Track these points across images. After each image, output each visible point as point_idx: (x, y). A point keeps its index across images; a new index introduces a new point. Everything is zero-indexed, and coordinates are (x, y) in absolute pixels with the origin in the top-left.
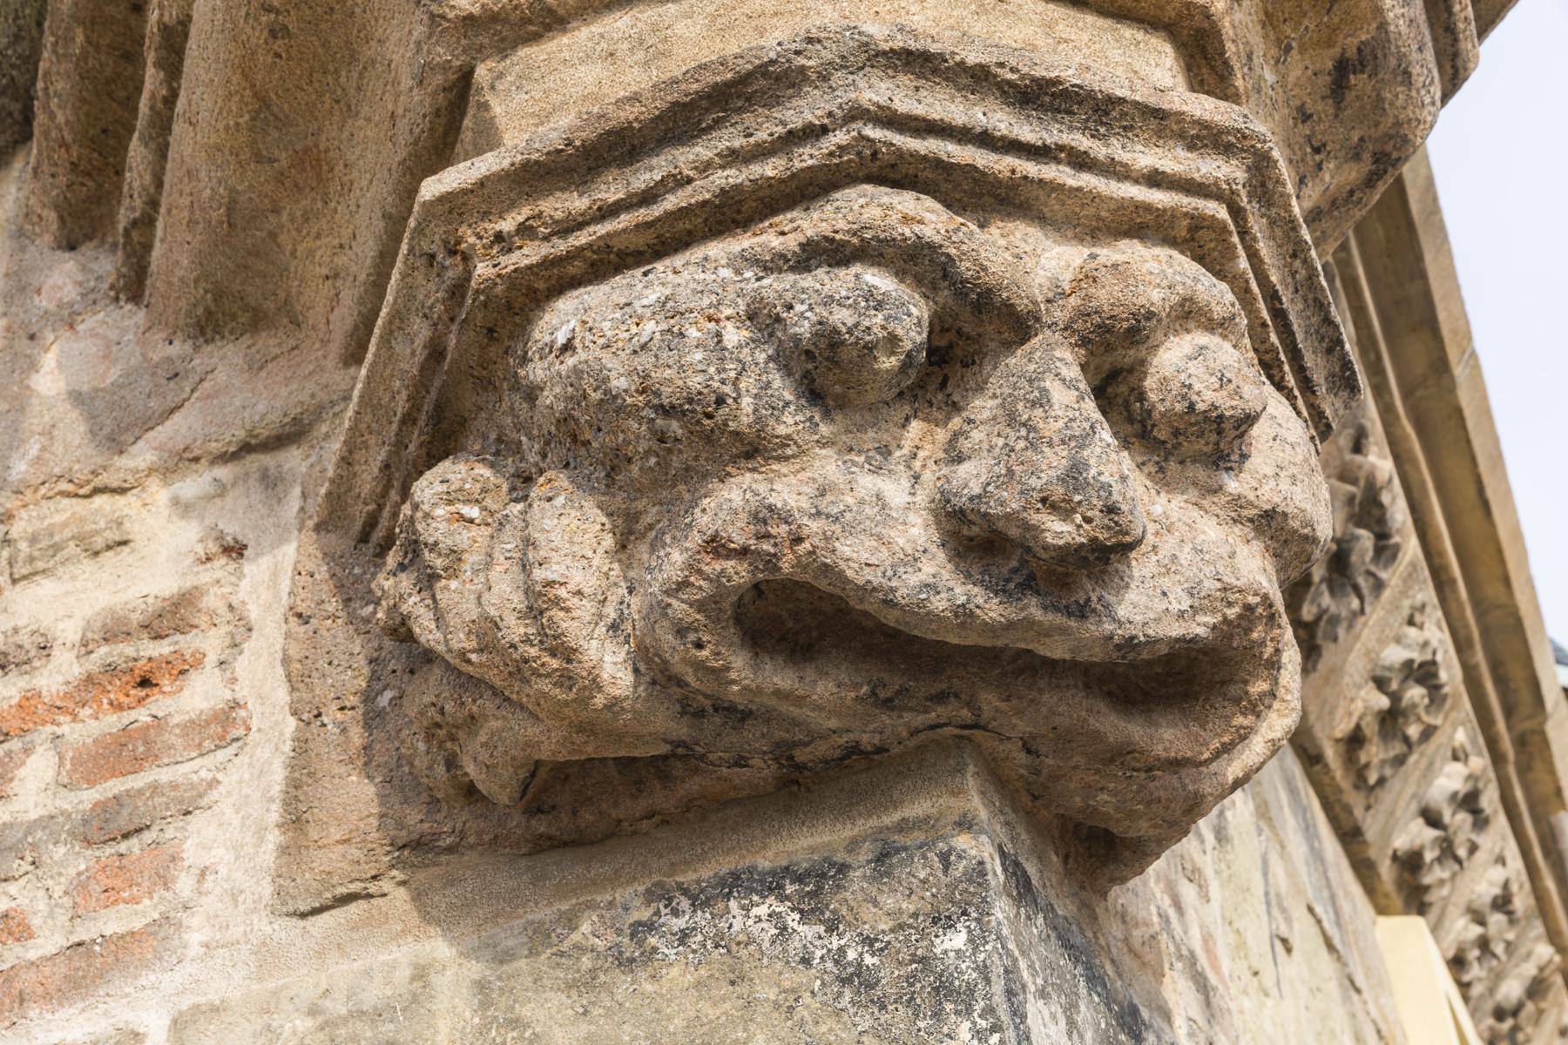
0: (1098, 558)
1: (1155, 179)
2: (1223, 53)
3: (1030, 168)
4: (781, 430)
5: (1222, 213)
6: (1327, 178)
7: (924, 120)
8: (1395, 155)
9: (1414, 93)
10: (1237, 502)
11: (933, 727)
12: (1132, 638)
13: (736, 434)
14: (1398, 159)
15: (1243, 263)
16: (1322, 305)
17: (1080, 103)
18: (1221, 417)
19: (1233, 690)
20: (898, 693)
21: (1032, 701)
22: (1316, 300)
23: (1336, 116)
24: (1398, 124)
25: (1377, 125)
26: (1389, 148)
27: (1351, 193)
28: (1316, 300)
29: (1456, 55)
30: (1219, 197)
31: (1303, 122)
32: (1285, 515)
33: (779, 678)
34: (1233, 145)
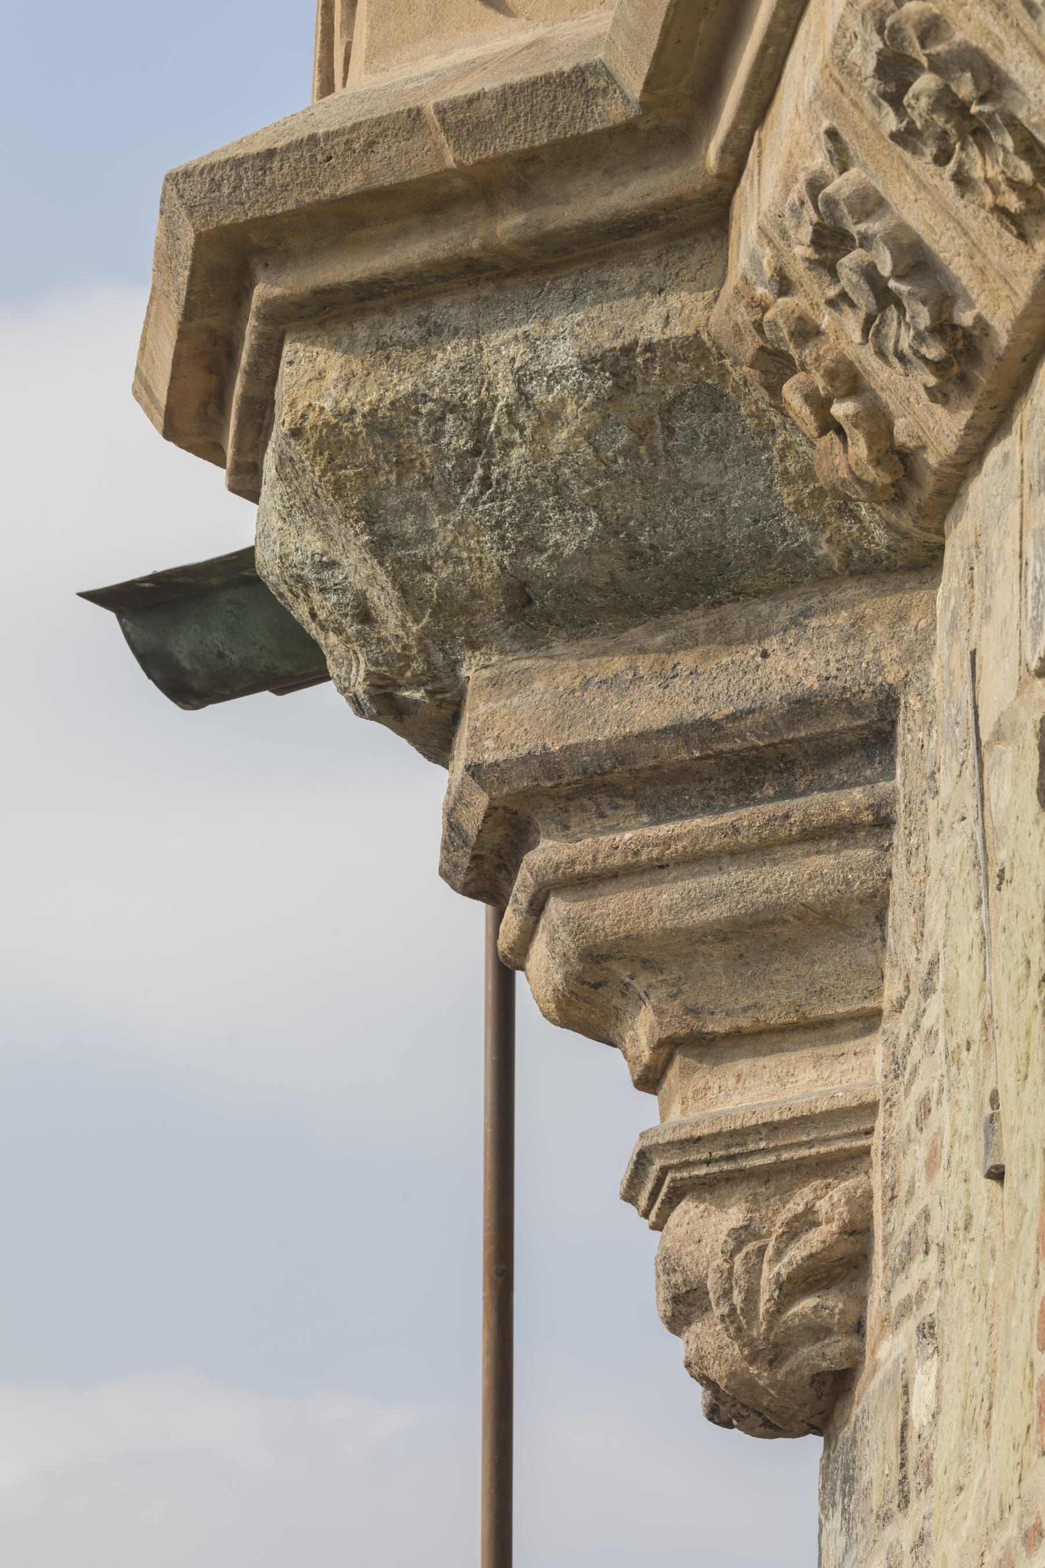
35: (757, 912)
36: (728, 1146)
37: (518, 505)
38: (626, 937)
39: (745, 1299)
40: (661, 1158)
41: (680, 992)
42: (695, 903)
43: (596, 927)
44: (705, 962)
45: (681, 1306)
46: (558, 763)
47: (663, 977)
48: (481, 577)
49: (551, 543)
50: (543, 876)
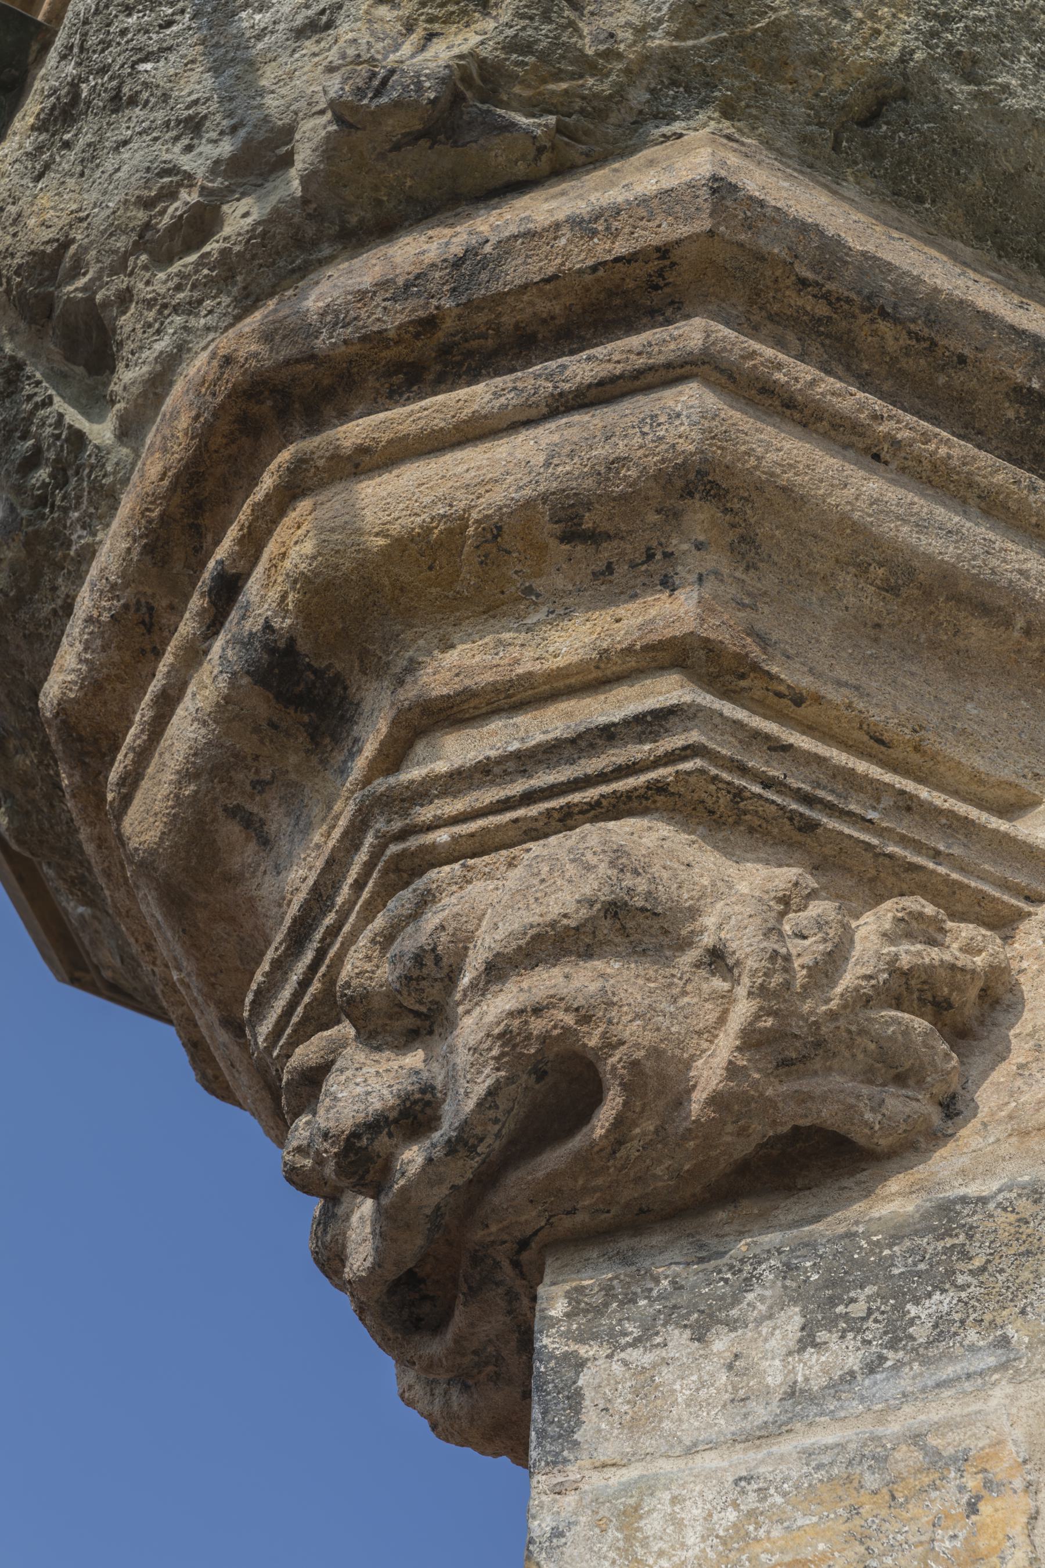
0: (356, 1154)
1: (359, 886)
2: (449, 696)
3: (323, 969)
4: (328, 1238)
5: (394, 849)
6: (685, 547)
7: (281, 1016)
8: (692, 476)
9: (640, 453)
10: (473, 986)
11: (516, 1264)
12: (449, 1141)
13: (329, 1259)
14: (698, 472)
15: (442, 836)
16: (554, 746)
17: (311, 909)
18: (406, 977)
19: (591, 1056)
20: (466, 1281)
21: (493, 1210)
22: (544, 752)
23: (622, 538)
24: (655, 478)
25: (647, 498)
26: (680, 483)
27: (726, 511)
28: (544, 752)
29: (669, 366)
30: (385, 846)
31: (611, 573)
32: (498, 953)
33: (449, 1336)
34: (362, 821)
35: (991, 584)
36: (818, 785)
37: (994, 20)
38: (784, 489)
39: (829, 954)
40: (703, 733)
41: (754, 608)
42: (913, 519)
43: (753, 450)
44: (821, 600)
45: (607, 923)
46: (846, 263)
47: (744, 577)
48: (857, 48)
49: (1000, 80)
50: (724, 350)
